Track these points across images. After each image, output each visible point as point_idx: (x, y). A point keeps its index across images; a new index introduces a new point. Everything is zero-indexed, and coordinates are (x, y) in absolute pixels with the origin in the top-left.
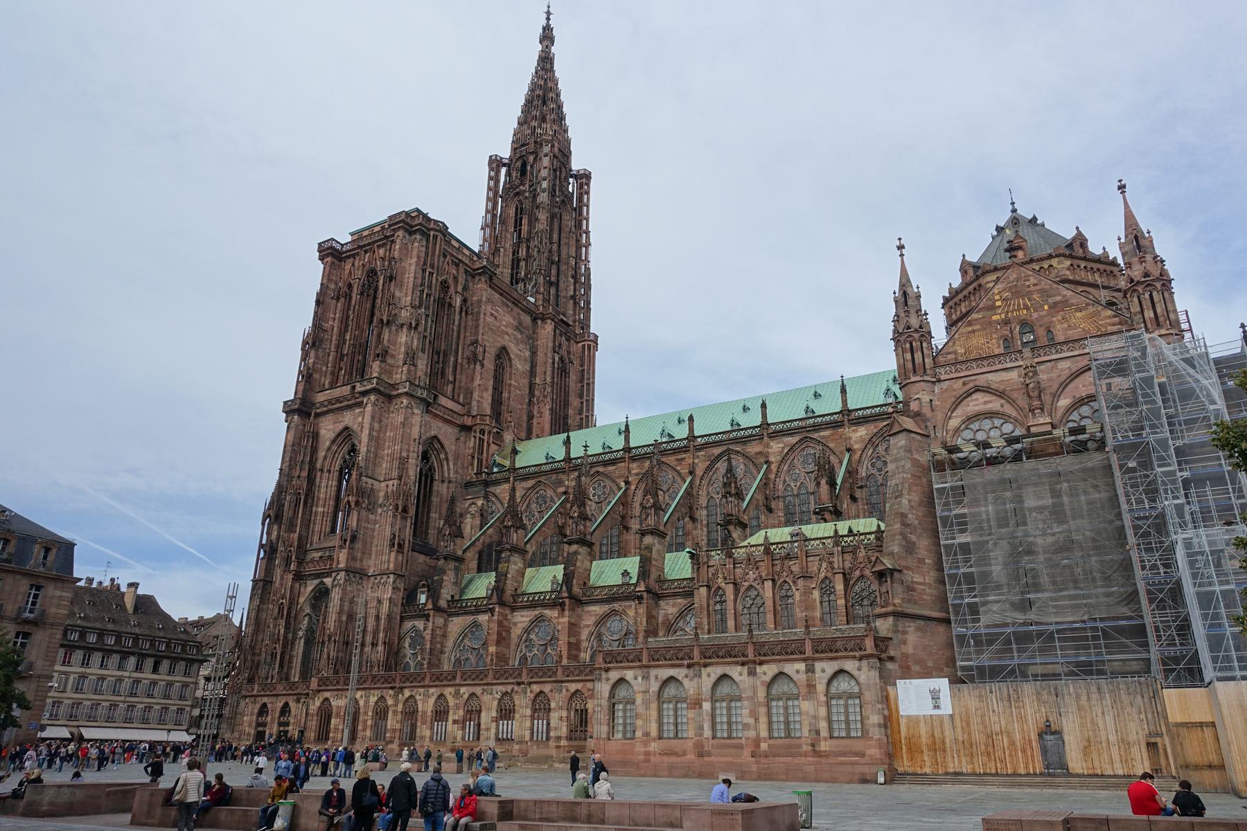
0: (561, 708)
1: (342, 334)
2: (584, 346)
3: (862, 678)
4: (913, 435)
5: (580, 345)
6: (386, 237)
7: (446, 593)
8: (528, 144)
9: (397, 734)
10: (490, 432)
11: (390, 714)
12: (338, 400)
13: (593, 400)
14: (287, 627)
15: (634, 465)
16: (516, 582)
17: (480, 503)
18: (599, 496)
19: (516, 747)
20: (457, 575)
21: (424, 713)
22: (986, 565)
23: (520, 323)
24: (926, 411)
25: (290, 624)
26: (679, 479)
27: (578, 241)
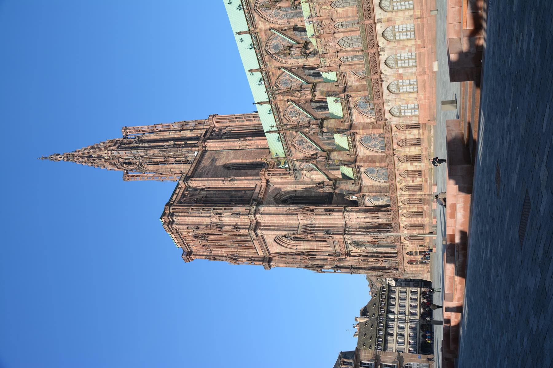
0: (405, 134)
1: (229, 247)
2: (216, 122)
6: (177, 232)
12: (261, 246)
16: (343, 155)
17: (304, 172)
18: (297, 114)
19: (424, 153)
26: (284, 74)
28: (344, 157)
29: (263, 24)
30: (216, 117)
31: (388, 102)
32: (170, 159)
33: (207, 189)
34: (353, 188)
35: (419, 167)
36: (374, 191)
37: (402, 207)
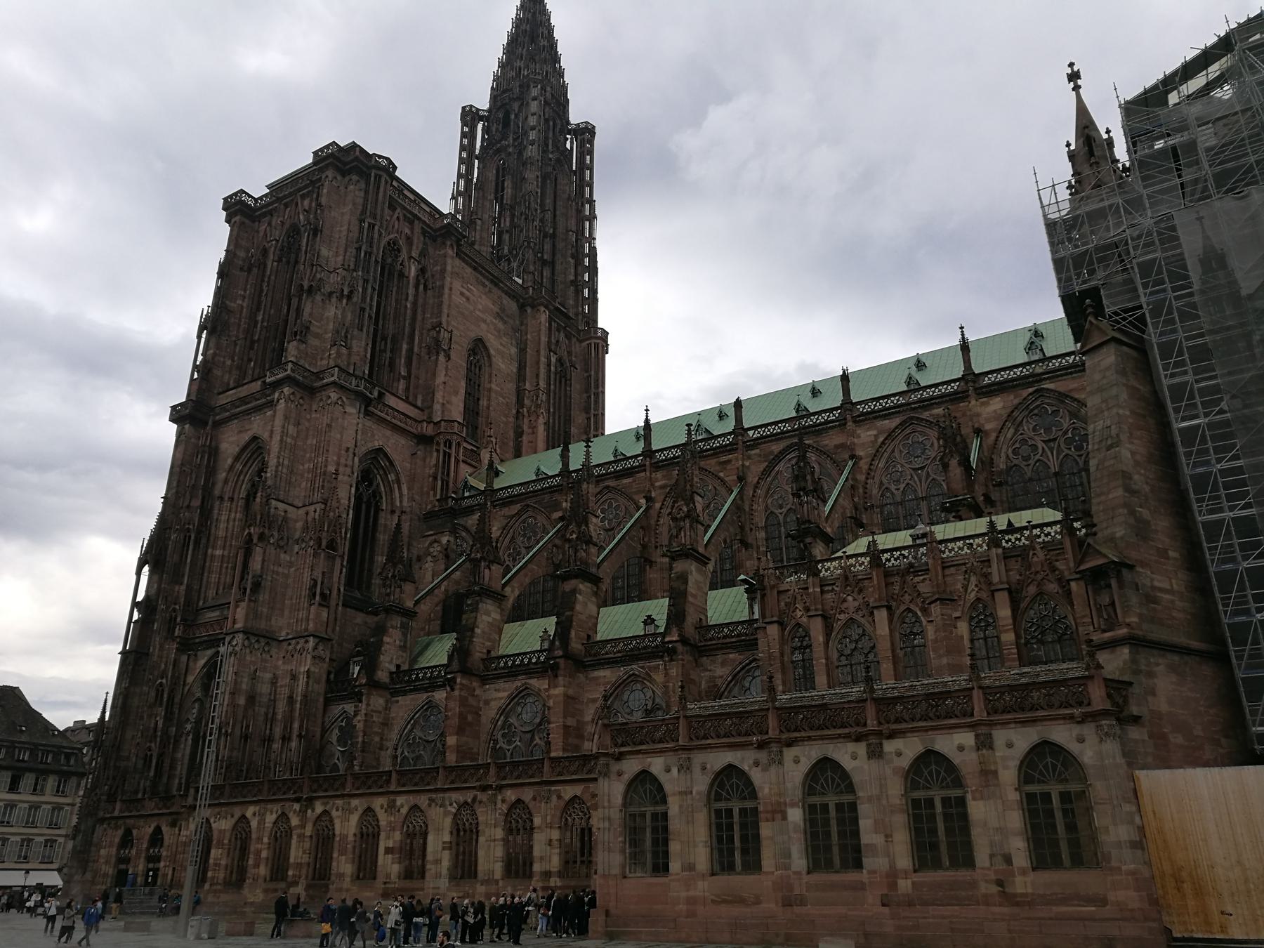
5: (585, 344)
7: (389, 660)
8: (512, 90)
9: (304, 871)
10: (459, 444)
12: (243, 400)
14: (168, 718)
15: (659, 475)
16: (489, 640)
17: (444, 540)
20: (405, 635)
21: (344, 837)
23: (503, 309)
25: (172, 713)
26: (723, 491)
27: (580, 211)
28: (481, 640)
29: (869, 439)
32: (508, 219)
33: (423, 281)
34: (387, 665)
35: (433, 871)
37: (309, 811)
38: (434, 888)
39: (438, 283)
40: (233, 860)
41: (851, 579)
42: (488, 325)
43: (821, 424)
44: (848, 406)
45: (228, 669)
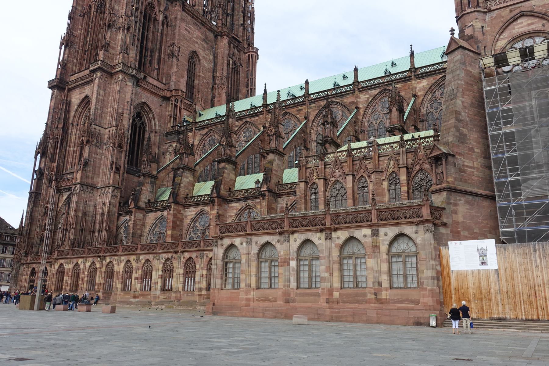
0: (202, 269)
3: (419, 239)
4: (467, 52)
5: (247, 55)
7: (144, 198)
9: (102, 287)
10: (181, 101)
11: (98, 274)
12: (81, 79)
13: (255, 89)
16: (187, 189)
17: (174, 145)
18: (247, 137)
19: (173, 295)
20: (152, 187)
21: (118, 272)
22: (528, 149)
23: (206, 37)
24: (478, 35)
26: (298, 123)
28: (184, 189)
29: (365, 99)
30: (255, 56)
31: (247, 243)
33: (166, 23)
34: (144, 199)
35: (154, 287)
36: (136, 226)
37: (104, 261)
38: (154, 294)
39: (173, 24)
40: (73, 282)
41: (338, 162)
42: (199, 45)
43: (344, 92)
44: (356, 83)
45: (74, 199)
